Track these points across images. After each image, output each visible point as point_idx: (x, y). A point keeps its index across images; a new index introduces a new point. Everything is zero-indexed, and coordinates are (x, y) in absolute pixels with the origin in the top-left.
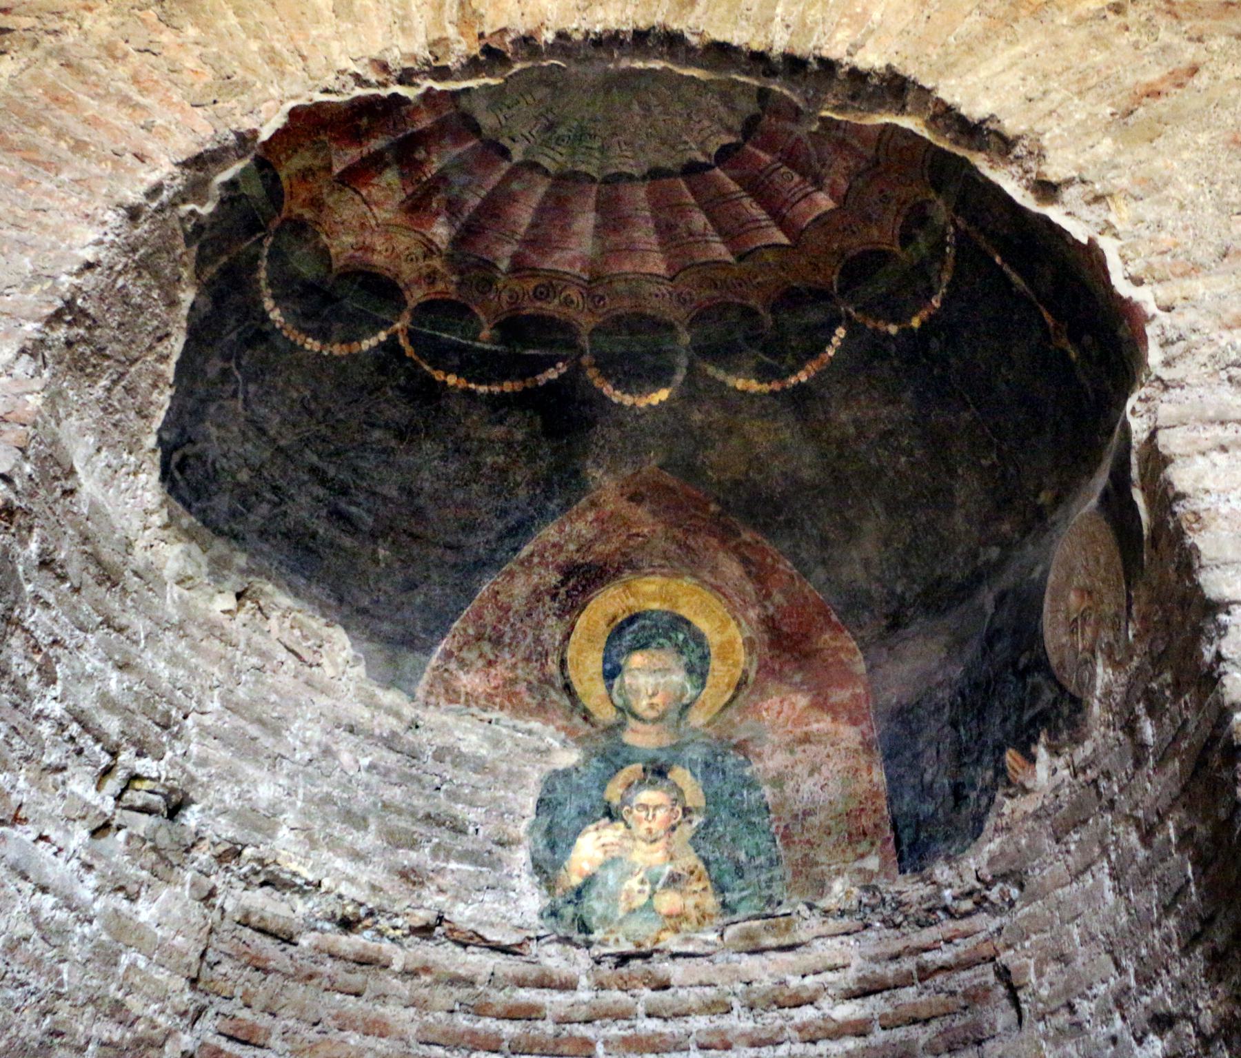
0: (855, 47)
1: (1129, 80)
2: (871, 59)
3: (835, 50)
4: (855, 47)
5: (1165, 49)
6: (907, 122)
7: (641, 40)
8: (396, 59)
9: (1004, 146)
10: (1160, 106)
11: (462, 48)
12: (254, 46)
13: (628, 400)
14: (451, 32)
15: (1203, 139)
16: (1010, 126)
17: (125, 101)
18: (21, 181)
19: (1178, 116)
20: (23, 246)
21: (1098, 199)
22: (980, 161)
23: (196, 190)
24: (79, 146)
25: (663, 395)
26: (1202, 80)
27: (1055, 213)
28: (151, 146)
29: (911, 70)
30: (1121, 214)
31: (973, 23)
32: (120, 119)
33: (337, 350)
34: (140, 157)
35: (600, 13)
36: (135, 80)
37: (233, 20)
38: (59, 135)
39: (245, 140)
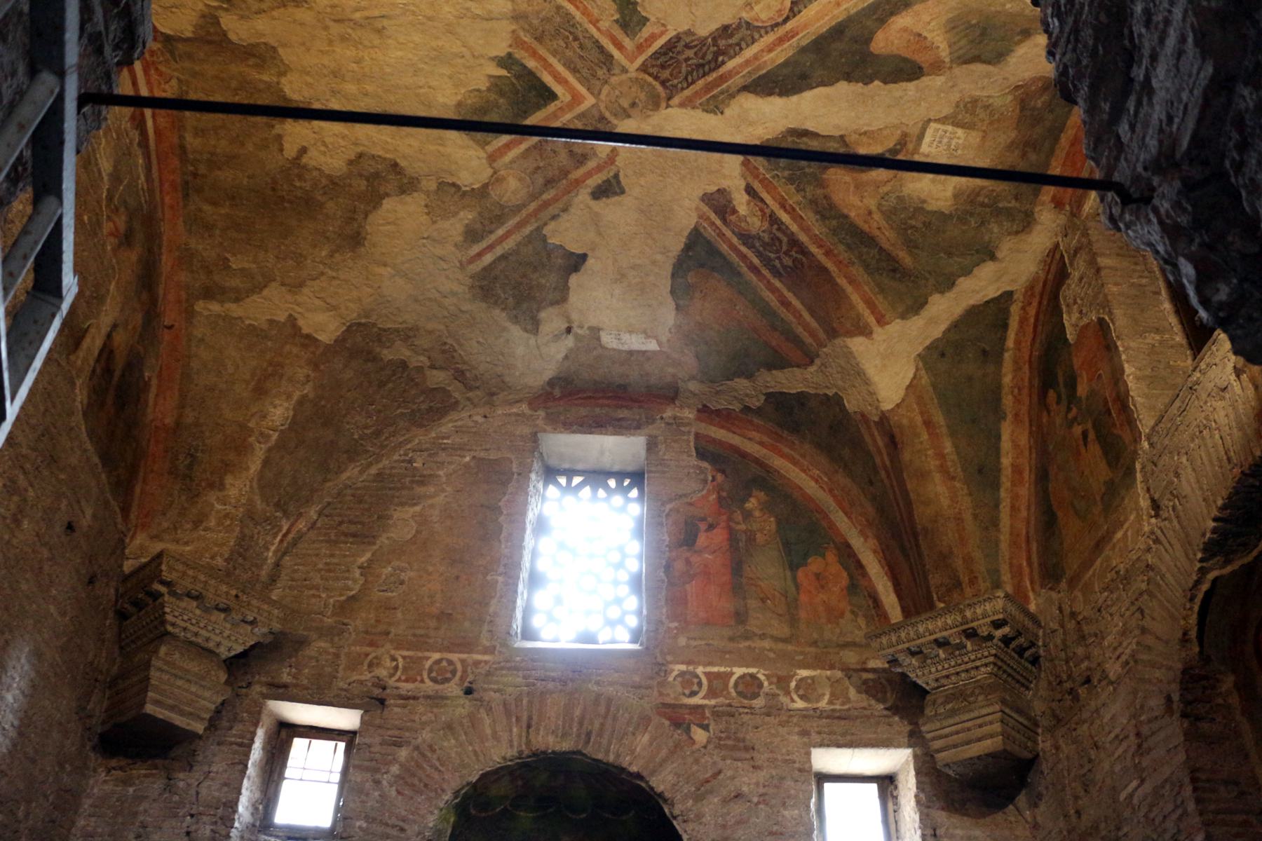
0: (630, 764)
1: (701, 778)
2: (634, 769)
3: (625, 765)
4: (630, 764)
5: (715, 763)
6: (643, 785)
7: (574, 753)
8: (508, 756)
9: (665, 801)
10: (708, 786)
11: (526, 752)
12: (470, 748)
13: (574, 816)
14: (524, 747)
15: (716, 800)
16: (667, 795)
17: (436, 769)
18: (412, 798)
19: (711, 792)
20: (415, 822)
21: (685, 821)
22: (661, 802)
23: (456, 798)
24: (426, 785)
25: (584, 815)
26: (721, 777)
27: (675, 823)
28: (445, 786)
29: (644, 774)
30: (690, 826)
31: (664, 753)
32: (436, 776)
33: (490, 813)
34: (443, 790)
35: (564, 745)
36: (438, 759)
37: (464, 737)
38: (420, 780)
39: (468, 784)
